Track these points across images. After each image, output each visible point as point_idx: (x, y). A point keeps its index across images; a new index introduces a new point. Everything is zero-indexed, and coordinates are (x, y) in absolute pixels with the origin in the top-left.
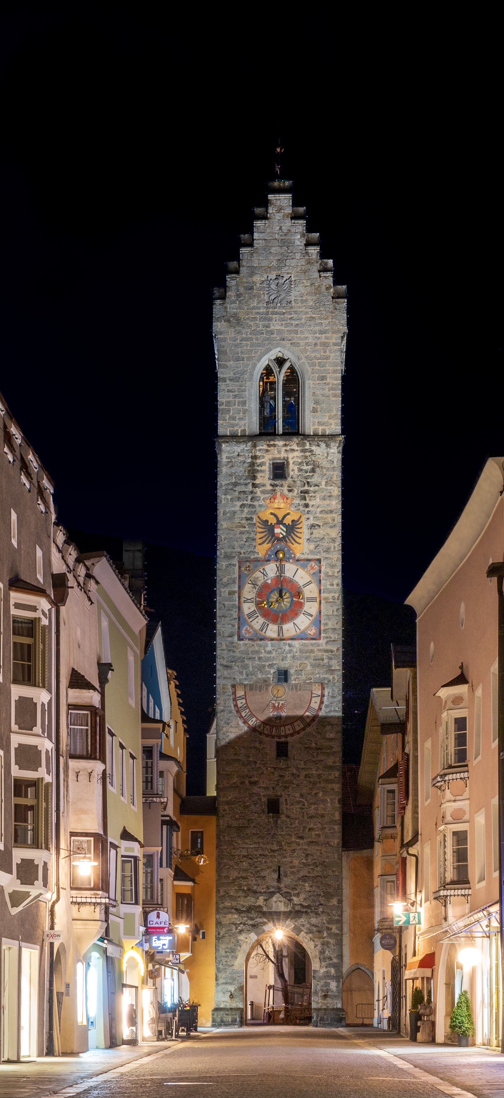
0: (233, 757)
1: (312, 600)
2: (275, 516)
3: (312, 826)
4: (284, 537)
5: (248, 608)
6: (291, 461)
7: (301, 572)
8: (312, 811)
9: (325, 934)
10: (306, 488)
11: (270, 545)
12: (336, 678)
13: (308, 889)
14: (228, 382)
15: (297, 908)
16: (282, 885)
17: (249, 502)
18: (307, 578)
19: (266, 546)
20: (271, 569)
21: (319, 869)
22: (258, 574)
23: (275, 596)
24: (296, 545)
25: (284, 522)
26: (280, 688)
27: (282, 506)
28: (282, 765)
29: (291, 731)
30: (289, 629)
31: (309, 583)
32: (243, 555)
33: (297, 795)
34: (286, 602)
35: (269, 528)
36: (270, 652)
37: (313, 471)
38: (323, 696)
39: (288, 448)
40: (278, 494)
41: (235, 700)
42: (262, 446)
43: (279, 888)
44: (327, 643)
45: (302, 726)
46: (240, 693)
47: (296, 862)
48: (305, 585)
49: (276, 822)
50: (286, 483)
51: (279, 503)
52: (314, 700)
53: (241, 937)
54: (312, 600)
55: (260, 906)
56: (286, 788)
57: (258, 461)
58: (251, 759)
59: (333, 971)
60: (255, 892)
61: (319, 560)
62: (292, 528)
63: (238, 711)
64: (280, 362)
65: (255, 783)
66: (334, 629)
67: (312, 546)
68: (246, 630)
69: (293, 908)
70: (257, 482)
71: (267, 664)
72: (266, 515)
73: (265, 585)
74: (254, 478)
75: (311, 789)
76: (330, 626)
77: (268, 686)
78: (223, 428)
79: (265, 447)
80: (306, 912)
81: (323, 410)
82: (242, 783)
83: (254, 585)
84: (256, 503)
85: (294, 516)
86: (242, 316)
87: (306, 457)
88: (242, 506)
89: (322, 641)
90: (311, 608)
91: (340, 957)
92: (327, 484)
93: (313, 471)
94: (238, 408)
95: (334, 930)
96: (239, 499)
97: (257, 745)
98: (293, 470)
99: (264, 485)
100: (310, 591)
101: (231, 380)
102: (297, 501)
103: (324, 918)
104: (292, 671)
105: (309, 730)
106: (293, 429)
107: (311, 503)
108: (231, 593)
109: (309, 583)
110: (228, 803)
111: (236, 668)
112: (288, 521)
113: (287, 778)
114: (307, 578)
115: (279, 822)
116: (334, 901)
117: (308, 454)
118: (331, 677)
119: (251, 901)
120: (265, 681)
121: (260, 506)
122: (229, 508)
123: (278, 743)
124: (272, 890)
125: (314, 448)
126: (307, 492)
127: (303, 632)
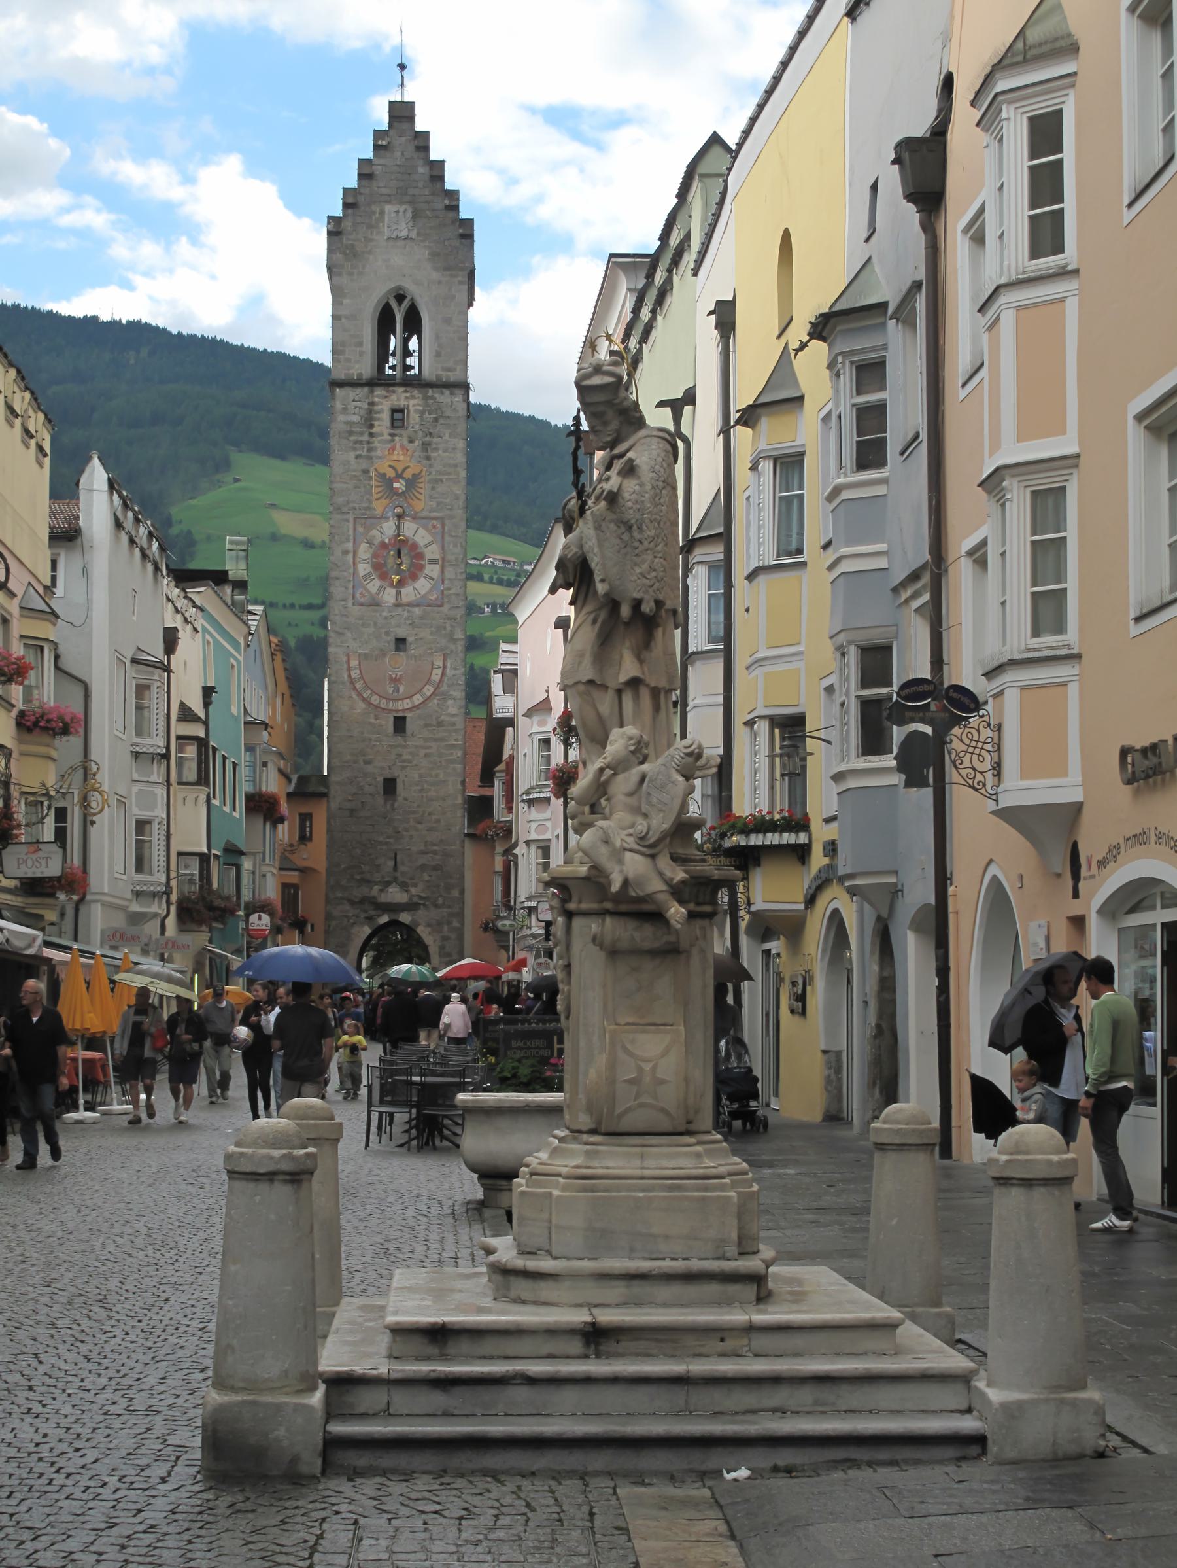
1: (432, 561)
4: (403, 493)
6: (411, 408)
7: (422, 531)
8: (432, 794)
9: (446, 928)
10: (428, 439)
11: (387, 501)
12: (460, 648)
13: (427, 878)
14: (343, 320)
15: (415, 900)
16: (398, 874)
17: (365, 453)
19: (384, 502)
21: (438, 857)
22: (374, 532)
24: (416, 501)
27: (401, 458)
28: (399, 740)
30: (408, 594)
31: (432, 543)
33: (416, 776)
35: (387, 482)
36: (386, 618)
37: (436, 420)
38: (444, 667)
39: (408, 395)
40: (398, 446)
41: (349, 669)
42: (379, 391)
43: (395, 879)
45: (421, 700)
46: (354, 663)
47: (414, 849)
48: (426, 546)
49: (393, 805)
51: (398, 454)
52: (435, 672)
53: (355, 930)
54: (432, 561)
55: (374, 897)
56: (403, 768)
57: (377, 408)
58: (366, 735)
60: (369, 882)
62: (412, 483)
63: (352, 682)
66: (458, 595)
67: (434, 504)
69: (410, 899)
70: (374, 430)
72: (385, 467)
73: (383, 545)
74: (372, 426)
77: (384, 655)
80: (424, 905)
83: (371, 543)
84: (373, 454)
87: (428, 405)
88: (357, 457)
90: (433, 570)
92: (450, 436)
93: (436, 420)
95: (456, 924)
96: (355, 449)
97: (372, 720)
98: (414, 419)
99: (382, 435)
100: (433, 552)
101: (346, 317)
103: (445, 911)
104: (410, 639)
107: (433, 455)
108: (346, 552)
109: (432, 543)
111: (349, 635)
112: (408, 474)
113: (406, 756)
115: (396, 805)
116: (455, 893)
118: (453, 647)
119: (365, 891)
120: (382, 650)
121: (380, 458)
123: (395, 718)
125: (437, 396)
126: (429, 444)
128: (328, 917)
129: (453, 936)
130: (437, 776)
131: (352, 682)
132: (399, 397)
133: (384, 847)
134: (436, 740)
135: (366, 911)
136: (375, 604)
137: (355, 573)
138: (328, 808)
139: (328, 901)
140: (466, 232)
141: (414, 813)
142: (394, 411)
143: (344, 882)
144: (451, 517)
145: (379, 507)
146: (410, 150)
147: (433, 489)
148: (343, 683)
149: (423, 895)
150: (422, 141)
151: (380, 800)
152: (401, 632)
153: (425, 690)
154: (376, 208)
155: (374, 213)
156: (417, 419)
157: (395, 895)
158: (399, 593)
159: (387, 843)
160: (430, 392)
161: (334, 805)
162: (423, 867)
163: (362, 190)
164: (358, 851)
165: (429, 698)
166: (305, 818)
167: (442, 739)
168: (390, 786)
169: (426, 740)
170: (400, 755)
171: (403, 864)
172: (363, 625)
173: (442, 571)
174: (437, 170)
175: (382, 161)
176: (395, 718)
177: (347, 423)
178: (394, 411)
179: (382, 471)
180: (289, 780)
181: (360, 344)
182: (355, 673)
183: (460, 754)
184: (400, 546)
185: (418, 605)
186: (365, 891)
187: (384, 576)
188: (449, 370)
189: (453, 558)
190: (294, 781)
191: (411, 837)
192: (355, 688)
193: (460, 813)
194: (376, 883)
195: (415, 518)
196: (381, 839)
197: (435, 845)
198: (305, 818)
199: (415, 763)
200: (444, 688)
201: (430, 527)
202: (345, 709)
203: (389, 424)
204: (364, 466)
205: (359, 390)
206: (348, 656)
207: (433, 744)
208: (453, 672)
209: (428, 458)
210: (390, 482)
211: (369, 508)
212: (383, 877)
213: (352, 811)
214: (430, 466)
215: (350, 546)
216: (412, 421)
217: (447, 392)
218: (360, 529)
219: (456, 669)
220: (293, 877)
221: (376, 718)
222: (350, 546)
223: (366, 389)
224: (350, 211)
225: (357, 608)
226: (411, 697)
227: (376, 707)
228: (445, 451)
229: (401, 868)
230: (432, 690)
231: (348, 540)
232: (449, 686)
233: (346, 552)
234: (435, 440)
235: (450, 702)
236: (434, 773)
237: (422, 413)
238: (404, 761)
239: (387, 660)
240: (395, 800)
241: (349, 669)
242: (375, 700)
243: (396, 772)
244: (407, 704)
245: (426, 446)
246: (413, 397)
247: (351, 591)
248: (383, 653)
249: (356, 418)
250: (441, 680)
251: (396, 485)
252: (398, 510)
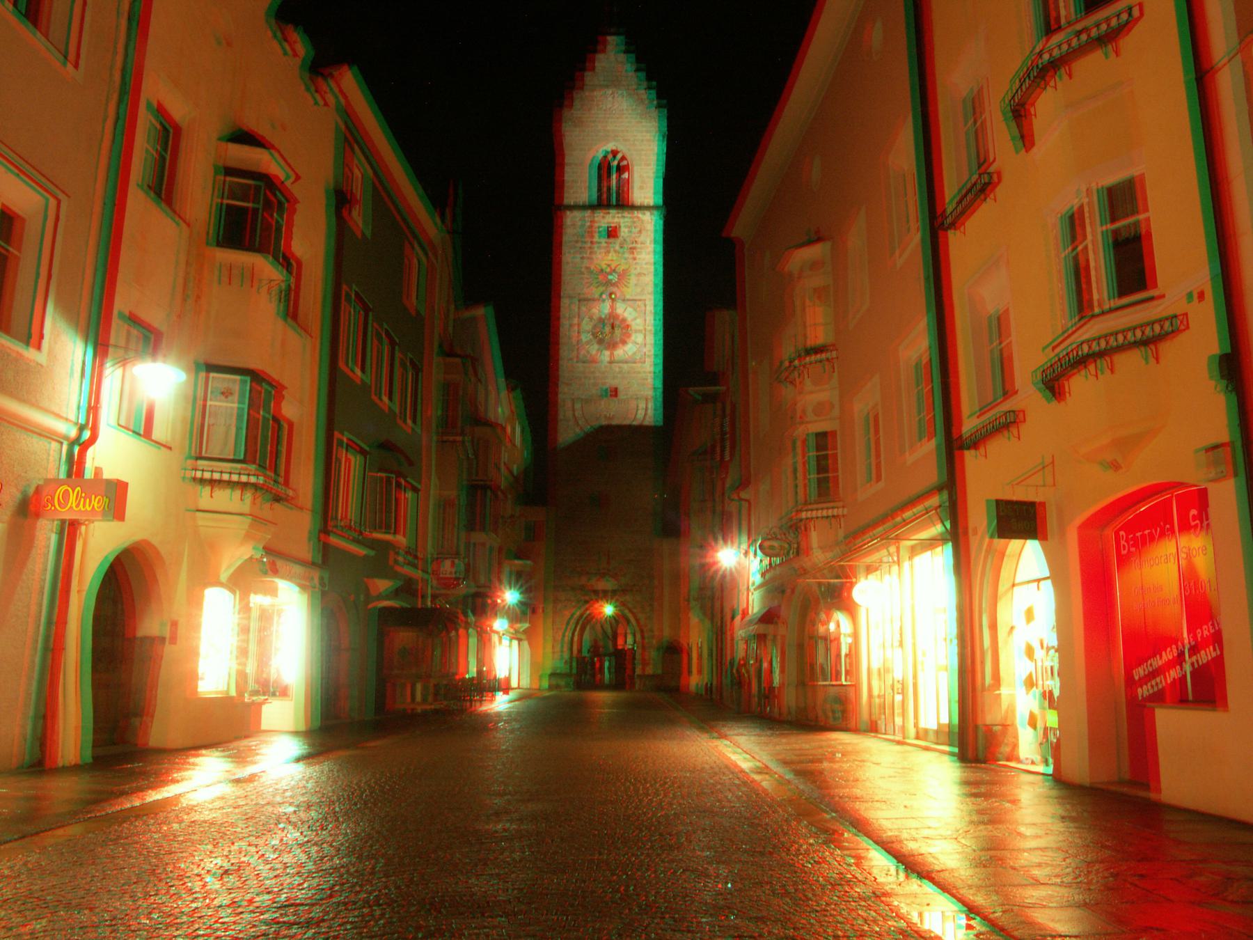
7: (629, 309)
23: (607, 329)
34: (618, 332)
37: (640, 232)
42: (599, 214)
46: (578, 406)
54: (640, 331)
62: (623, 275)
64: (615, 153)
73: (601, 320)
78: (569, 199)
81: (647, 183)
83: (591, 318)
90: (639, 338)
94: (579, 183)
98: (624, 232)
102: (626, 255)
106: (624, 203)
112: (620, 269)
114: (634, 314)
122: (570, 259)
187: (600, 342)
217: (648, 213)
218: (584, 309)
233: (571, 325)
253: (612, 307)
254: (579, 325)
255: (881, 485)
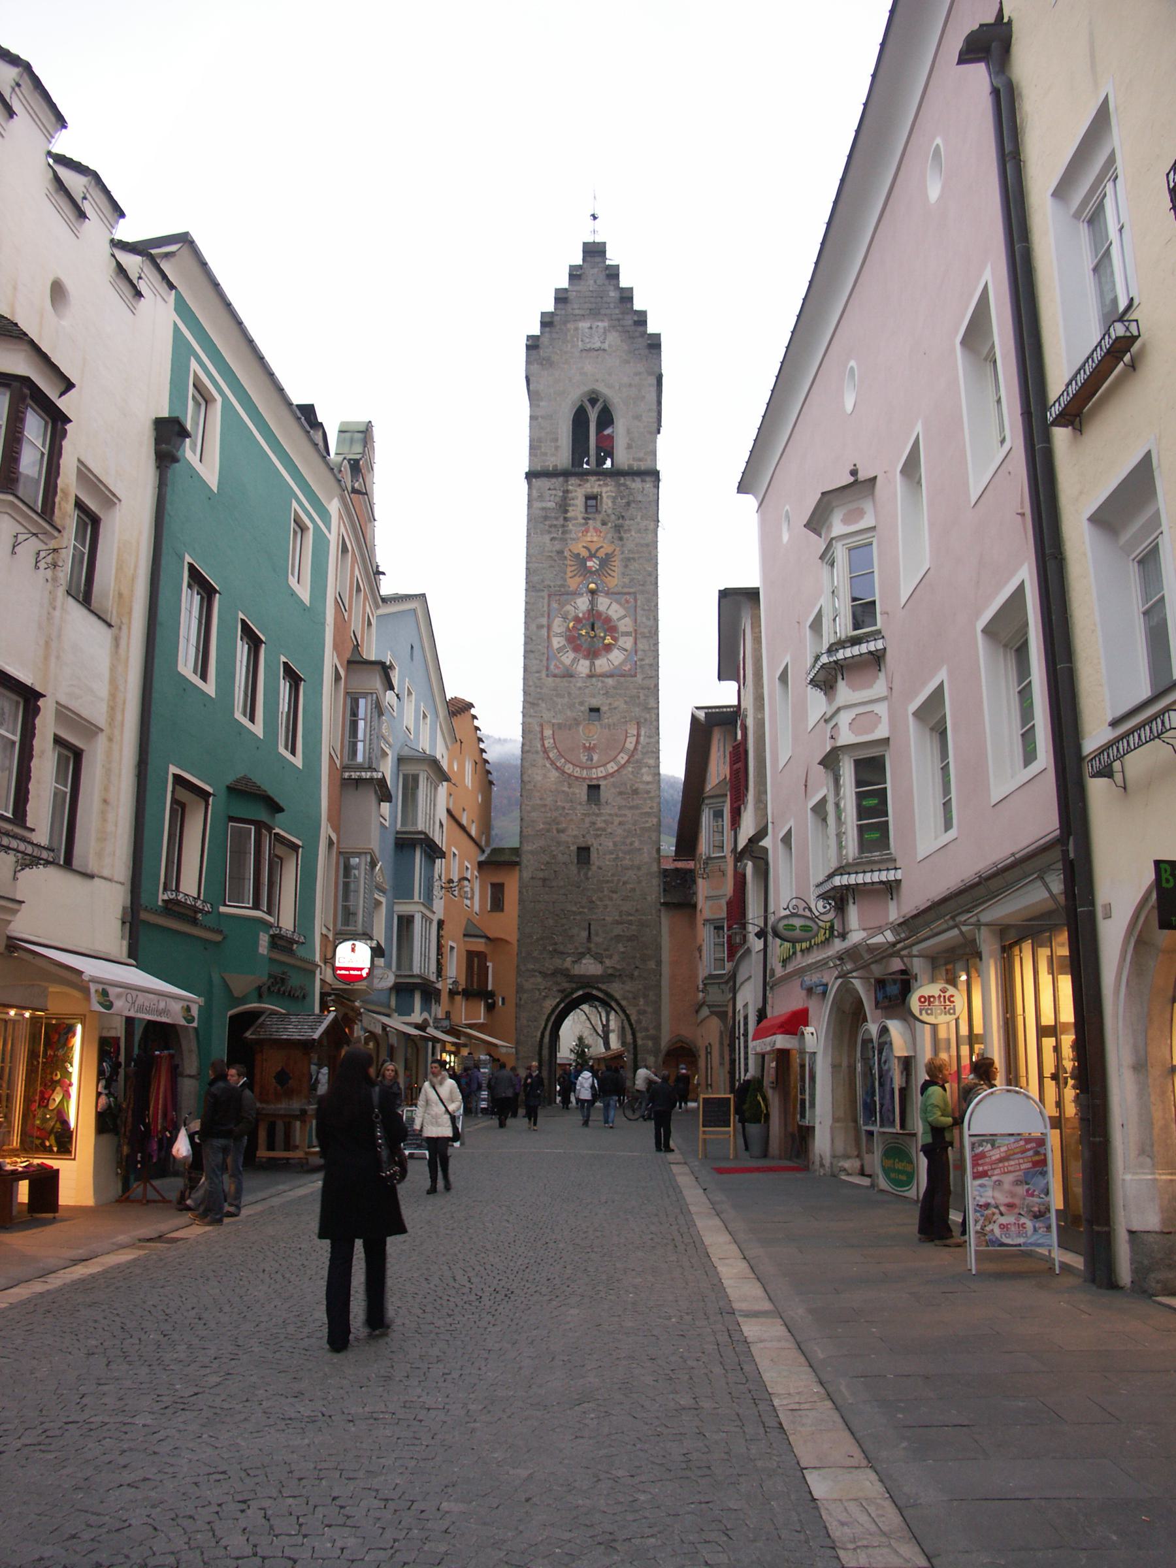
0: (539, 802)
1: (627, 634)
2: (589, 550)
3: (625, 879)
5: (557, 642)
7: (615, 606)
8: (627, 862)
9: (642, 1002)
13: (622, 950)
15: (610, 971)
18: (622, 612)
19: (578, 579)
20: (583, 603)
22: (568, 607)
25: (598, 554)
26: (591, 727)
27: (595, 539)
29: (604, 774)
30: (602, 664)
31: (625, 616)
32: (552, 589)
33: (611, 844)
35: (581, 561)
36: (580, 688)
37: (628, 504)
38: (638, 735)
42: (573, 480)
43: (589, 949)
44: (643, 679)
45: (616, 768)
46: (548, 732)
48: (619, 619)
49: (586, 874)
50: (599, 517)
51: (592, 536)
54: (627, 634)
55: (567, 969)
59: (650, 1043)
60: (562, 953)
61: (635, 593)
62: (605, 562)
63: (545, 751)
65: (562, 831)
67: (627, 580)
68: (555, 665)
71: (577, 701)
73: (577, 620)
74: (566, 511)
75: (627, 837)
76: (647, 661)
77: (578, 724)
79: (578, 482)
82: (548, 831)
83: (565, 618)
84: (568, 536)
85: (607, 549)
86: (555, 358)
88: (552, 539)
89: (639, 677)
91: (658, 1027)
93: (628, 504)
96: (550, 532)
97: (566, 789)
98: (607, 504)
99: (576, 519)
104: (604, 709)
105: (624, 772)
107: (625, 536)
108: (540, 627)
109: (625, 616)
110: (532, 852)
112: (601, 554)
113: (600, 825)
114: (622, 612)
115: (590, 874)
116: (652, 965)
117: (622, 488)
119: (557, 962)
123: (589, 786)
124: (580, 950)
125: (628, 483)
126: (622, 526)
127: (616, 668)
128: (520, 989)
129: (650, 1009)
130: (631, 844)
131: (545, 751)
132: (592, 485)
133: (578, 917)
134: (631, 808)
135: (558, 984)
136: (569, 675)
137: (549, 645)
138: (521, 878)
139: (519, 973)
140: (654, 344)
141: (608, 882)
142: (588, 498)
143: (535, 954)
144: (642, 592)
145: (573, 583)
146: (601, 279)
147: (626, 566)
148: (537, 752)
149: (618, 967)
150: (613, 273)
151: (574, 869)
152: (595, 703)
153: (619, 758)
154: (570, 326)
155: (568, 330)
156: (610, 504)
157: (589, 967)
158: (592, 664)
159: (580, 913)
160: (622, 480)
161: (526, 875)
162: (618, 938)
163: (558, 312)
164: (551, 922)
165: (623, 766)
166: (498, 890)
167: (636, 807)
168: (584, 853)
169: (620, 808)
170: (594, 823)
171: (597, 935)
172: (558, 695)
173: (636, 643)
174: (627, 296)
175: (576, 288)
176: (589, 786)
177: (543, 509)
178: (588, 498)
179: (576, 552)
180: (483, 851)
181: (556, 440)
182: (548, 743)
183: (655, 820)
184: (594, 619)
185: (611, 676)
186: (557, 962)
187: (576, 649)
188: (640, 460)
189: (646, 630)
190: (488, 851)
191: (606, 907)
192: (548, 758)
193: (655, 882)
194: (569, 954)
195: (607, 594)
196: (574, 909)
197: (630, 915)
198: (498, 890)
199: (609, 830)
200: (638, 756)
201: (623, 601)
202: (539, 778)
203: (583, 510)
204: (558, 546)
205: (554, 480)
206: (542, 725)
207: (628, 812)
208: (648, 740)
209: (621, 539)
210: (584, 560)
211: (562, 586)
212: (576, 948)
213: (544, 880)
214: (623, 546)
215: (544, 621)
216: (605, 506)
217: (638, 479)
218: (555, 605)
219: (650, 737)
220: (479, 945)
221: (570, 786)
222: (544, 621)
223: (561, 479)
224: (547, 329)
225: (550, 679)
226: (604, 765)
227: (570, 775)
228: (639, 531)
229: (595, 939)
230: (626, 758)
231: (543, 616)
232: (643, 754)
233: (540, 627)
234: (627, 522)
235: (644, 770)
236: (628, 841)
237: (614, 498)
238: (598, 829)
239: (581, 728)
240: (589, 869)
241: (542, 739)
242: (569, 768)
243: (590, 841)
244: (601, 772)
245: (618, 528)
246: (606, 485)
247: (545, 662)
248: (577, 722)
249: (551, 505)
250: (635, 749)
251: (589, 564)
252: (592, 586)
253: (592, 602)
254: (549, 627)
255: (952, 834)
